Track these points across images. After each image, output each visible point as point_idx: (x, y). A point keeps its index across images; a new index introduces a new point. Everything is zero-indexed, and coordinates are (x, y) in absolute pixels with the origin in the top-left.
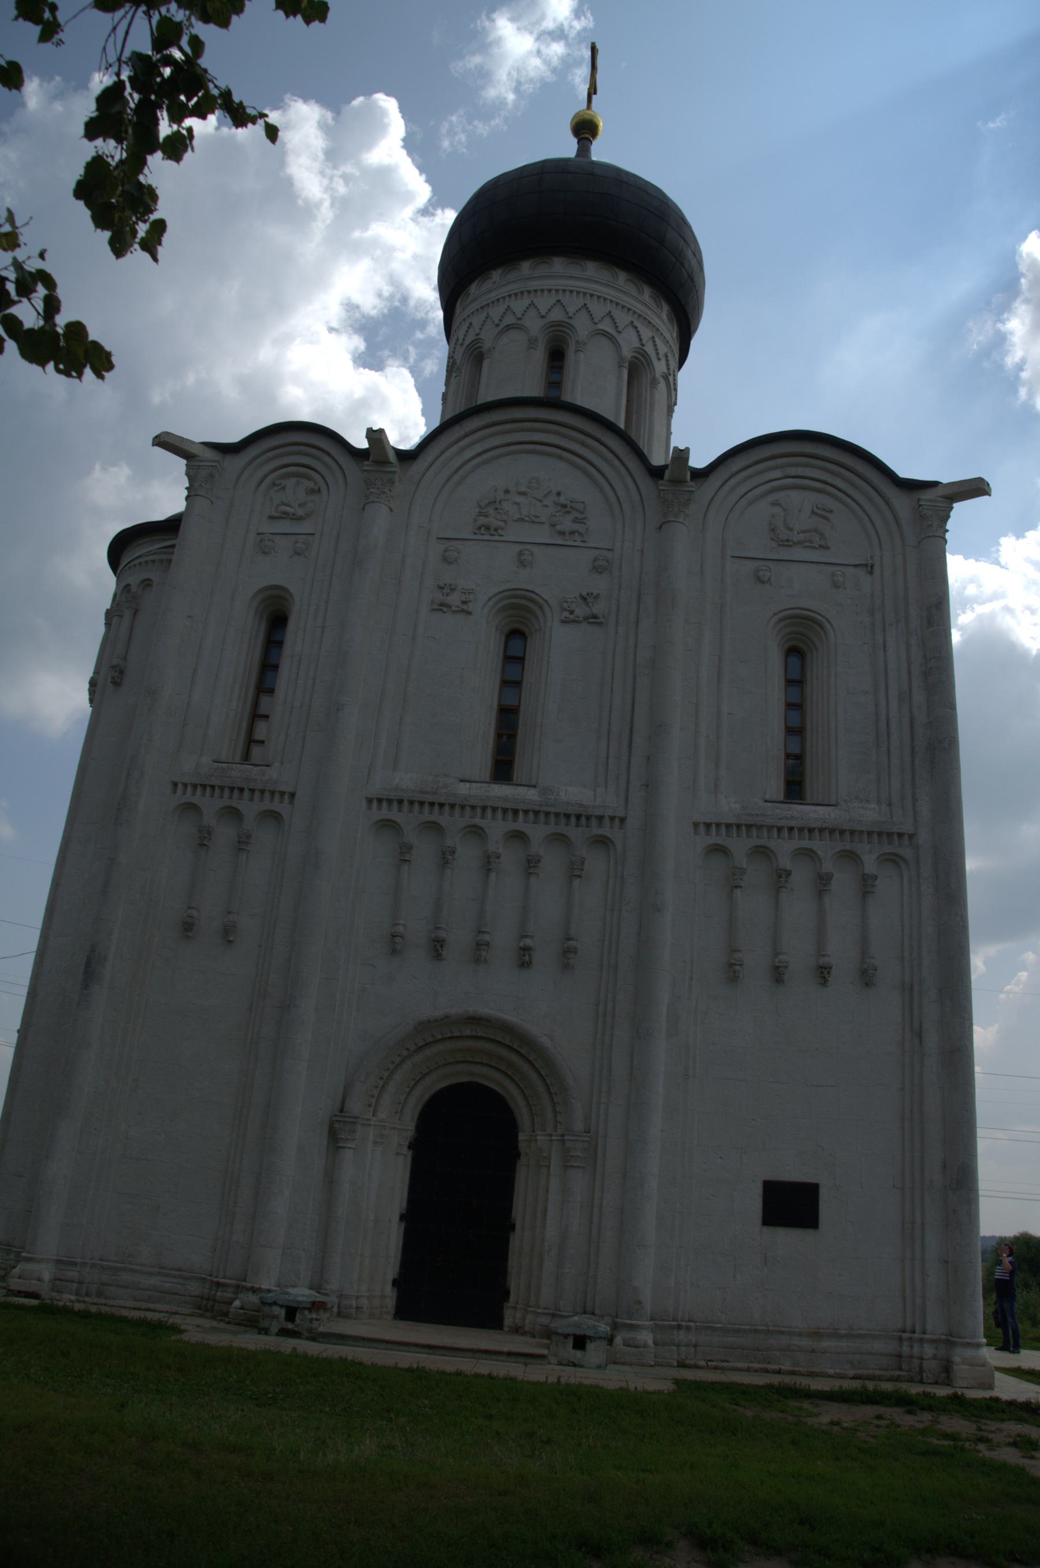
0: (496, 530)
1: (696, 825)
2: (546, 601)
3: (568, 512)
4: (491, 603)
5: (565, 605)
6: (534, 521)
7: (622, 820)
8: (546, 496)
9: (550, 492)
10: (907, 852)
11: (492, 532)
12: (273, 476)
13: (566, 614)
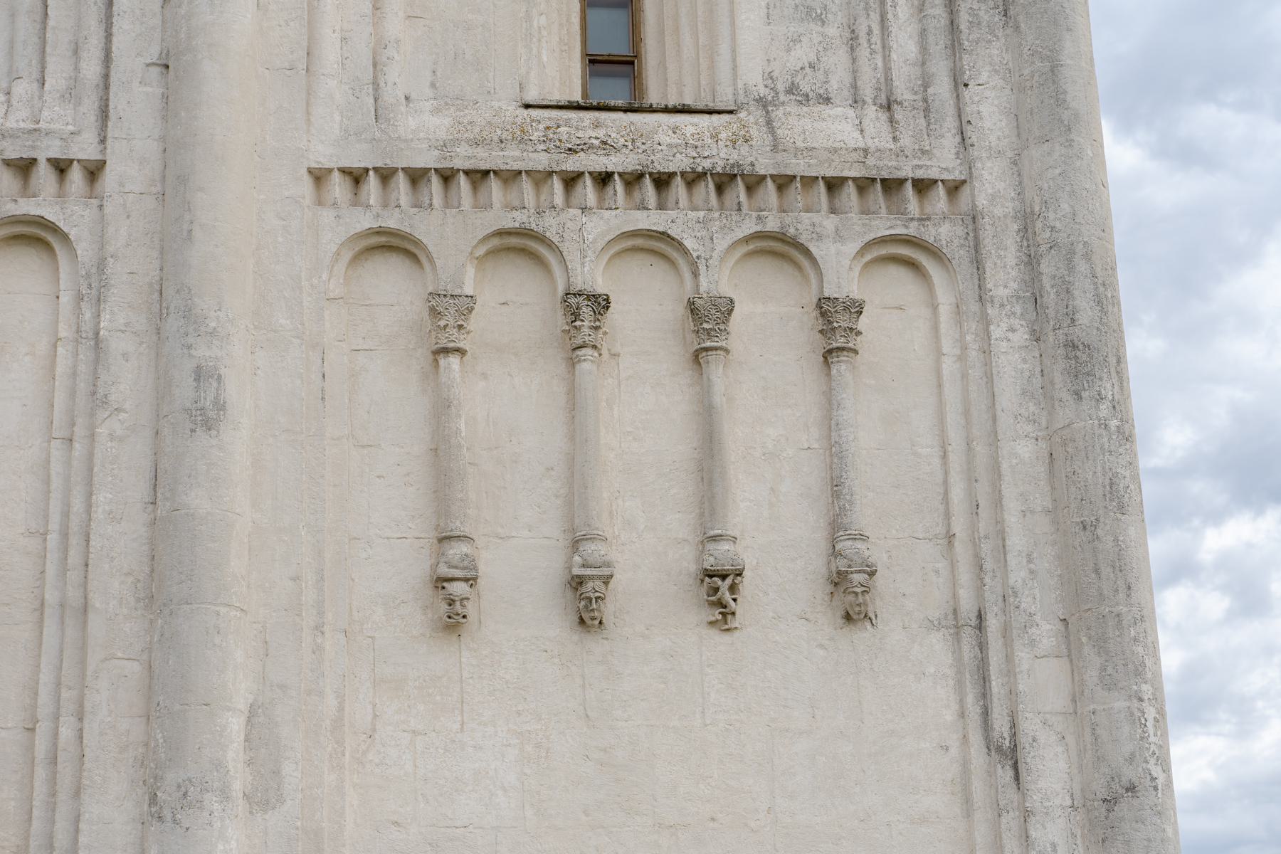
1: (319, 177)
7: (94, 172)
10: (945, 233)
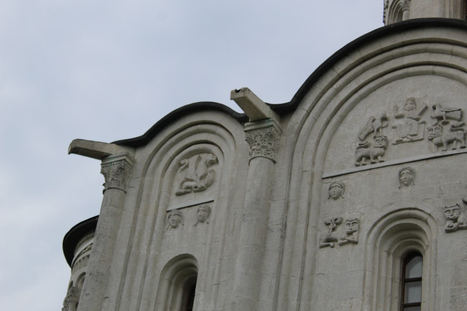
0: (376, 157)
2: (430, 215)
3: (445, 123)
4: (376, 229)
5: (448, 215)
6: (414, 139)
8: (422, 113)
9: (426, 108)
11: (372, 160)
12: (177, 158)
13: (449, 223)
